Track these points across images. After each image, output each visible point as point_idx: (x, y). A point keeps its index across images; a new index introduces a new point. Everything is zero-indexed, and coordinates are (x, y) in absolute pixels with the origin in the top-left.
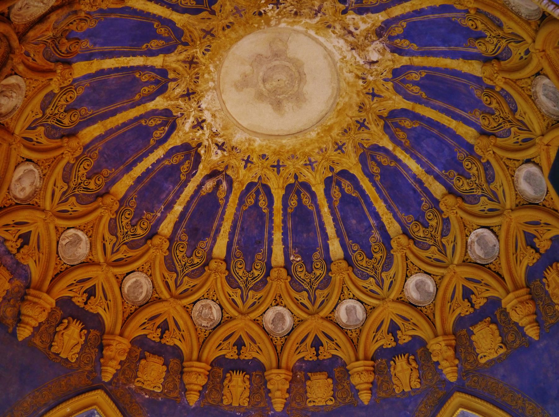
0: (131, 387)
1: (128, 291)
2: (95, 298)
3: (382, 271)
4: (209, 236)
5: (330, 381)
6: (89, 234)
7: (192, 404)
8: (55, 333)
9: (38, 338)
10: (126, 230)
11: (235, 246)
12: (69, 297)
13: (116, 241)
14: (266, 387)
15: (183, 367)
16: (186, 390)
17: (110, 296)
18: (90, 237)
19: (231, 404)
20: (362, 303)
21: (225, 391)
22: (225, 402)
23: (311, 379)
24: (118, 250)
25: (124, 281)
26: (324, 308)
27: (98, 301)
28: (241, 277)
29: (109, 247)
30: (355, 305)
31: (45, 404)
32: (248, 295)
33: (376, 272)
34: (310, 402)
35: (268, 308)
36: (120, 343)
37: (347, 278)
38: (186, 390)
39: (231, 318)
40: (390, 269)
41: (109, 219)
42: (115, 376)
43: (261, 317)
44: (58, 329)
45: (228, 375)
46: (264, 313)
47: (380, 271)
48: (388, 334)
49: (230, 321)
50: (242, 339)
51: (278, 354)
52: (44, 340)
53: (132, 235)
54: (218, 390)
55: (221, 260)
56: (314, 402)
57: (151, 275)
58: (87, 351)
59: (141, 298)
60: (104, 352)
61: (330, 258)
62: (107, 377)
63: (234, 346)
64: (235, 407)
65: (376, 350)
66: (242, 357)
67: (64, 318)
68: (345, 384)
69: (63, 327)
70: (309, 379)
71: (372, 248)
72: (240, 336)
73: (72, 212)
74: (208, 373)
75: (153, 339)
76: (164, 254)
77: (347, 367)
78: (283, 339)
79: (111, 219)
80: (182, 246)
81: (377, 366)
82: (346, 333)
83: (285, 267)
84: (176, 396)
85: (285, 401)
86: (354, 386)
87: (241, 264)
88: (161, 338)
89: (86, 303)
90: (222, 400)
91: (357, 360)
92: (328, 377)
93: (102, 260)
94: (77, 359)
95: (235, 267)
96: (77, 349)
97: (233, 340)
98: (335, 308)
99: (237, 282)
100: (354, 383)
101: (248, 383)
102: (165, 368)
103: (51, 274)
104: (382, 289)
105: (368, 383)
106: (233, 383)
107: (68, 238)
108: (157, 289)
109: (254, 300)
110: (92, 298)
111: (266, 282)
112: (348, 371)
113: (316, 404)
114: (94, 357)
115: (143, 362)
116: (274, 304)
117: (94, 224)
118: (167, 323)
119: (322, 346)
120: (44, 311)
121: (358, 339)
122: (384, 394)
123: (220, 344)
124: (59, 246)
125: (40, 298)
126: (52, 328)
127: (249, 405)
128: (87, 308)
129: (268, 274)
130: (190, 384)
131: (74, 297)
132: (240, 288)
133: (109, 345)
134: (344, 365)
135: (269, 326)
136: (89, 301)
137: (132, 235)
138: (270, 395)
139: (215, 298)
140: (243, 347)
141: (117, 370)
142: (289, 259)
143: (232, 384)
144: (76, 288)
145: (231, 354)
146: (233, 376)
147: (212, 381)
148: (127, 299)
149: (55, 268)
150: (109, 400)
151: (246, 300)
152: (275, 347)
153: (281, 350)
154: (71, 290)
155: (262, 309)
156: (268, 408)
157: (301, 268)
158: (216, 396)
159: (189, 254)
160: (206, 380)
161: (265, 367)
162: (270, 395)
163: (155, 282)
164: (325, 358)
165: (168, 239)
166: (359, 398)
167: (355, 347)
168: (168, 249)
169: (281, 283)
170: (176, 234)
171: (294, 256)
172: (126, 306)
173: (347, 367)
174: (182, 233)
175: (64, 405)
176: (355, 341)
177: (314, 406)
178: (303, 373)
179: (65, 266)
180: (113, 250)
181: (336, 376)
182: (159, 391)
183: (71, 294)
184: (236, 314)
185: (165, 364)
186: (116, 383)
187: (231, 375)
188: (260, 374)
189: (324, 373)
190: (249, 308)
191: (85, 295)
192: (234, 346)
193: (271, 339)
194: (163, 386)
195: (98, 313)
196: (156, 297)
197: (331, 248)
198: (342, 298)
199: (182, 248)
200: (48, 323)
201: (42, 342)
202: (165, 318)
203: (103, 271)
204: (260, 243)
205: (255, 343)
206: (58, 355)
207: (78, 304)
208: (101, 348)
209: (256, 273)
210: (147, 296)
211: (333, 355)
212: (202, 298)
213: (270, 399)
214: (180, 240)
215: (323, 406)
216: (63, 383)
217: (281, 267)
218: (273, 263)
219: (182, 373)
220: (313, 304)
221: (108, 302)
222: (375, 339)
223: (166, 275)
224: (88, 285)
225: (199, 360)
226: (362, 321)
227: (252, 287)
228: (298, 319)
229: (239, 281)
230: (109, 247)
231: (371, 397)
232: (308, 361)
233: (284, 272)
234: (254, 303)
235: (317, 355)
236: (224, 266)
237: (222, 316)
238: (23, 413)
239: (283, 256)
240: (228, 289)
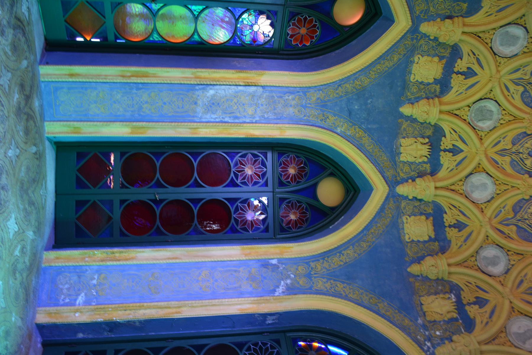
7: (401, 110)
22: (403, 141)
23: (427, 221)
43: (482, 170)
70: (427, 218)
90: (404, 138)
101: (420, 160)
113: (405, 225)
145: (446, 143)
150: (405, 32)
161: (434, 175)
176: (466, 264)
185: (436, 81)
208: (450, 17)
213: (407, 181)
220: (500, 223)
228: (484, 208)
235: (450, 226)
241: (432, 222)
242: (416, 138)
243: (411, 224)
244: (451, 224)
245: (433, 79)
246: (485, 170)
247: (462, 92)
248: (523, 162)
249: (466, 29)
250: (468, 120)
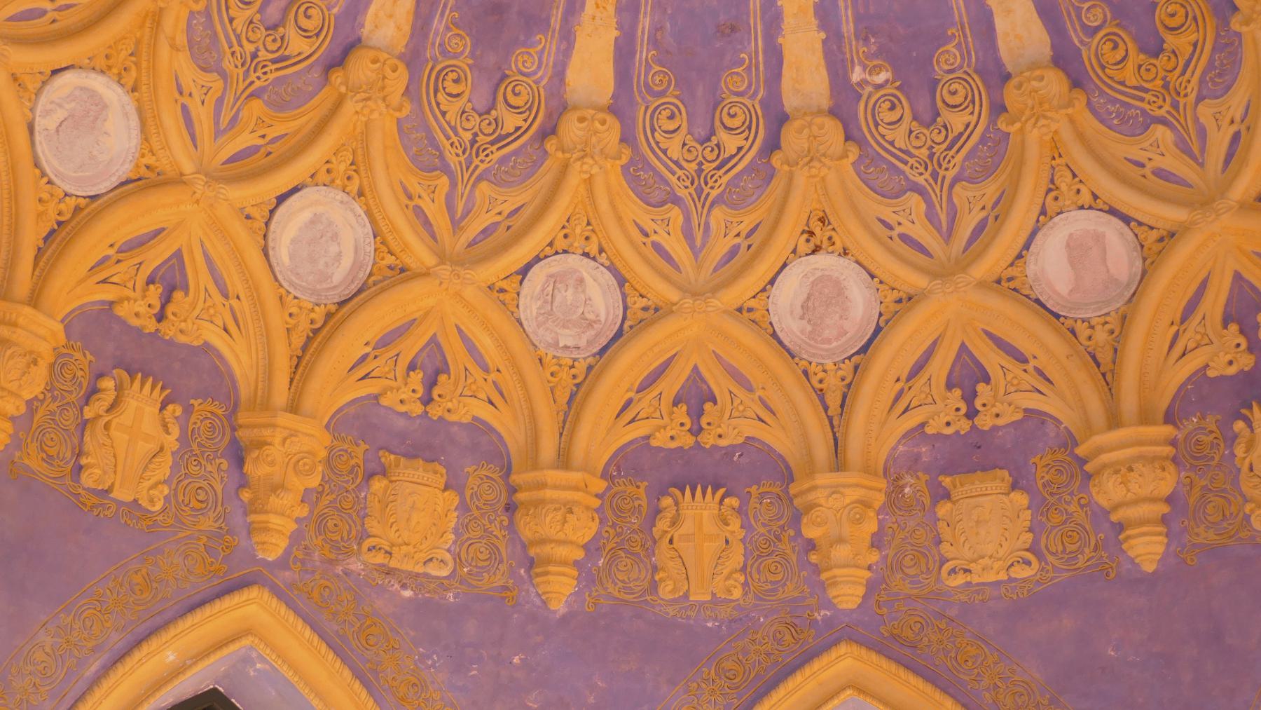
0: (352, 567)
1: (291, 257)
2: (187, 294)
3: (1200, 99)
4: (544, 25)
5: (1020, 499)
6: (130, 79)
7: (558, 606)
8: (83, 425)
9: (33, 447)
10: (250, 48)
11: (644, 53)
12: (103, 302)
13: (225, 89)
14: (799, 533)
15: (513, 490)
16: (531, 563)
17: (235, 283)
18: (134, 90)
19: (686, 596)
20: (1126, 219)
21: (663, 554)
22: (665, 591)
23: (954, 496)
24: (234, 120)
25: (273, 226)
26: (987, 246)
27: (200, 305)
28: (676, 163)
29: (203, 116)
30: (1101, 229)
31: (95, 649)
32: (707, 227)
33: (1175, 105)
34: (953, 571)
35: (785, 265)
36: (294, 433)
37: (1067, 134)
38: (531, 563)
39: (656, 310)
40: (1229, 88)
41: (185, 14)
42: (296, 538)
44: (88, 413)
45: (667, 502)
46: (772, 282)
47: (1192, 97)
48: (1225, 327)
49: (652, 322)
50: (704, 382)
51: (830, 419)
52: (52, 452)
53: (274, 61)
54: (638, 555)
55: (601, 109)
56: (966, 571)
57: (361, 194)
58: (194, 469)
59: (339, 273)
60: (248, 467)
61: (998, 63)
62: (273, 548)
63: (676, 403)
64: (702, 603)
65: (1184, 385)
66: (708, 440)
67: (100, 376)
68: (1071, 509)
69: (106, 405)
70: (947, 496)
71: (1160, 13)
72: (695, 369)
73: (55, 15)
74: (597, 503)
75: (403, 409)
76: (398, 115)
77: (1080, 451)
78: (848, 367)
79: (192, 14)
80: (453, 76)
81: (1186, 438)
82: (1073, 332)
83: (833, 112)
84: (501, 583)
85: (867, 574)
86: (1107, 513)
87: (671, 117)
88: (427, 400)
89: (160, 317)
90: (654, 586)
91: (1114, 421)
92: (1014, 486)
93: (188, 167)
94: (167, 498)
95: (653, 130)
96: (163, 468)
97: (671, 384)
98: (1027, 246)
99: (667, 183)
100: (1103, 501)
101: (735, 524)
102: (452, 498)
103: (31, 237)
104: (1201, 165)
105: (1153, 500)
106: (686, 527)
107: (60, 106)
108: (389, 238)
109: (731, 241)
110: (178, 295)
111: (771, 175)
112: (1083, 461)
113: (976, 579)
114: (219, 488)
115: (378, 484)
116: (803, 247)
117: (138, 42)
118: (439, 346)
119: (987, 379)
120: (35, 362)
121: (1116, 350)
122: (1211, 535)
123: (629, 402)
124: (38, 138)
125: (14, 325)
126: (71, 414)
127: (745, 594)
128: (169, 330)
129: (773, 144)
130: (543, 542)
131: (121, 301)
132: (676, 201)
133: (261, 444)
134: (1069, 442)
135: (791, 327)
136: (170, 309)
137: (274, 61)
138: (813, 558)
139: (593, 249)
140: (708, 406)
141: (298, 521)
142: (847, 79)
143: (683, 530)
144: (121, 272)
146: (683, 505)
147: (614, 526)
148: (291, 284)
149: (40, 215)
150: (292, 617)
151: (703, 245)
152: (821, 394)
153: (842, 406)
154: (104, 281)
155: (763, 269)
156: (812, 601)
157: (893, 108)
158: (634, 575)
159: (481, 104)
160: (595, 526)
161: (788, 467)
163: (378, 217)
164: (1000, 422)
165: (401, 57)
166: (1123, 551)
167: (1108, 379)
168: (407, 91)
169: (824, 171)
170: (426, 36)
171: (864, 67)
172: (294, 310)
173: (1080, 451)
174: (448, 28)
175: (154, 643)
176: (1105, 357)
177: (969, 584)
178: (924, 478)
179: (71, 202)
180: (217, 123)
181: (1040, 483)
182: (444, 573)
183: (107, 294)
184: (673, 295)
186: (303, 562)
187: (677, 504)
188: (777, 490)
189: (999, 472)
190: (715, 270)
191: (155, 292)
192: (676, 403)
193: (805, 373)
194: (457, 558)
195: (206, 344)
196: (390, 268)
197: (1000, 24)
198: (1051, 206)
199: (456, 81)
200: (54, 399)
201: (49, 459)
202: (430, 334)
203: (197, 202)
204: (733, 30)
205: (750, 389)
206: (106, 492)
207: (135, 322)
208: (238, 456)
209: (731, 143)
210: (357, 266)
211: (1026, 410)
212: (548, 251)
214: (444, 53)
215: (998, 584)
216: (138, 579)
217: (820, 112)
218: (790, 101)
219: (510, 508)
220: (948, 236)
221: (234, 302)
222: (1178, 349)
223: (414, 185)
224: (156, 256)
225: (564, 460)
226: (1128, 285)
227: (720, 196)
228: (896, 295)
229: (673, 179)
230: (203, 116)
231: (1168, 545)
232: (939, 436)
233: (832, 132)
234: (733, 252)
235: (972, 414)
236: (611, 132)
237: (625, 308)
238: (38, 681)
239: (824, 72)
240: (635, 210)
241: (957, 478)
242: (655, 542)
243: (968, 554)
244: (964, 410)
245: (446, 493)
246: (764, 290)
247: (494, 382)
248: (732, 157)
249: (281, 395)
250: (591, 360)
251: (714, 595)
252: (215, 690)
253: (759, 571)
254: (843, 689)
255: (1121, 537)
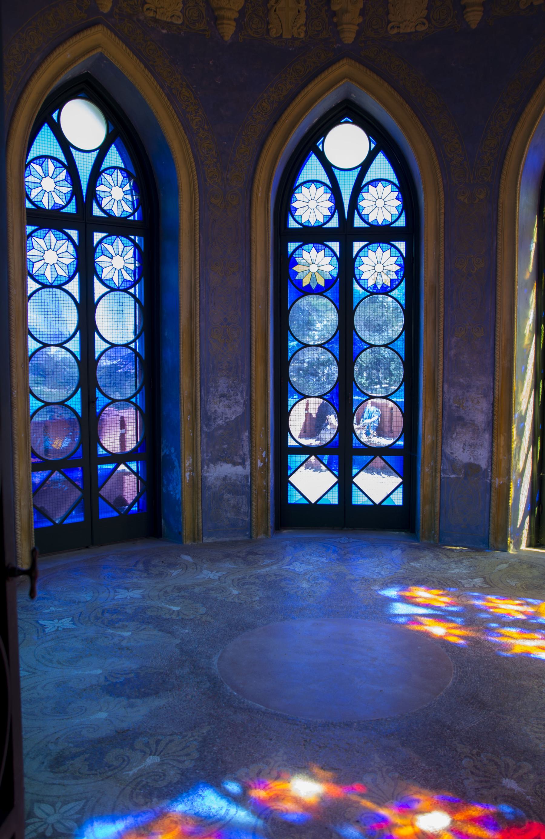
19: (281, 35)
22: (273, 33)
90: (268, 31)
113: (402, 31)
130: (221, 8)
138: (335, 20)
162: (335, 20)
177: (398, 33)
182: (180, 22)
215: (410, 34)
251: (293, 36)
252: (87, 73)
253: (312, 26)
254: (344, 78)
255: (464, 12)
